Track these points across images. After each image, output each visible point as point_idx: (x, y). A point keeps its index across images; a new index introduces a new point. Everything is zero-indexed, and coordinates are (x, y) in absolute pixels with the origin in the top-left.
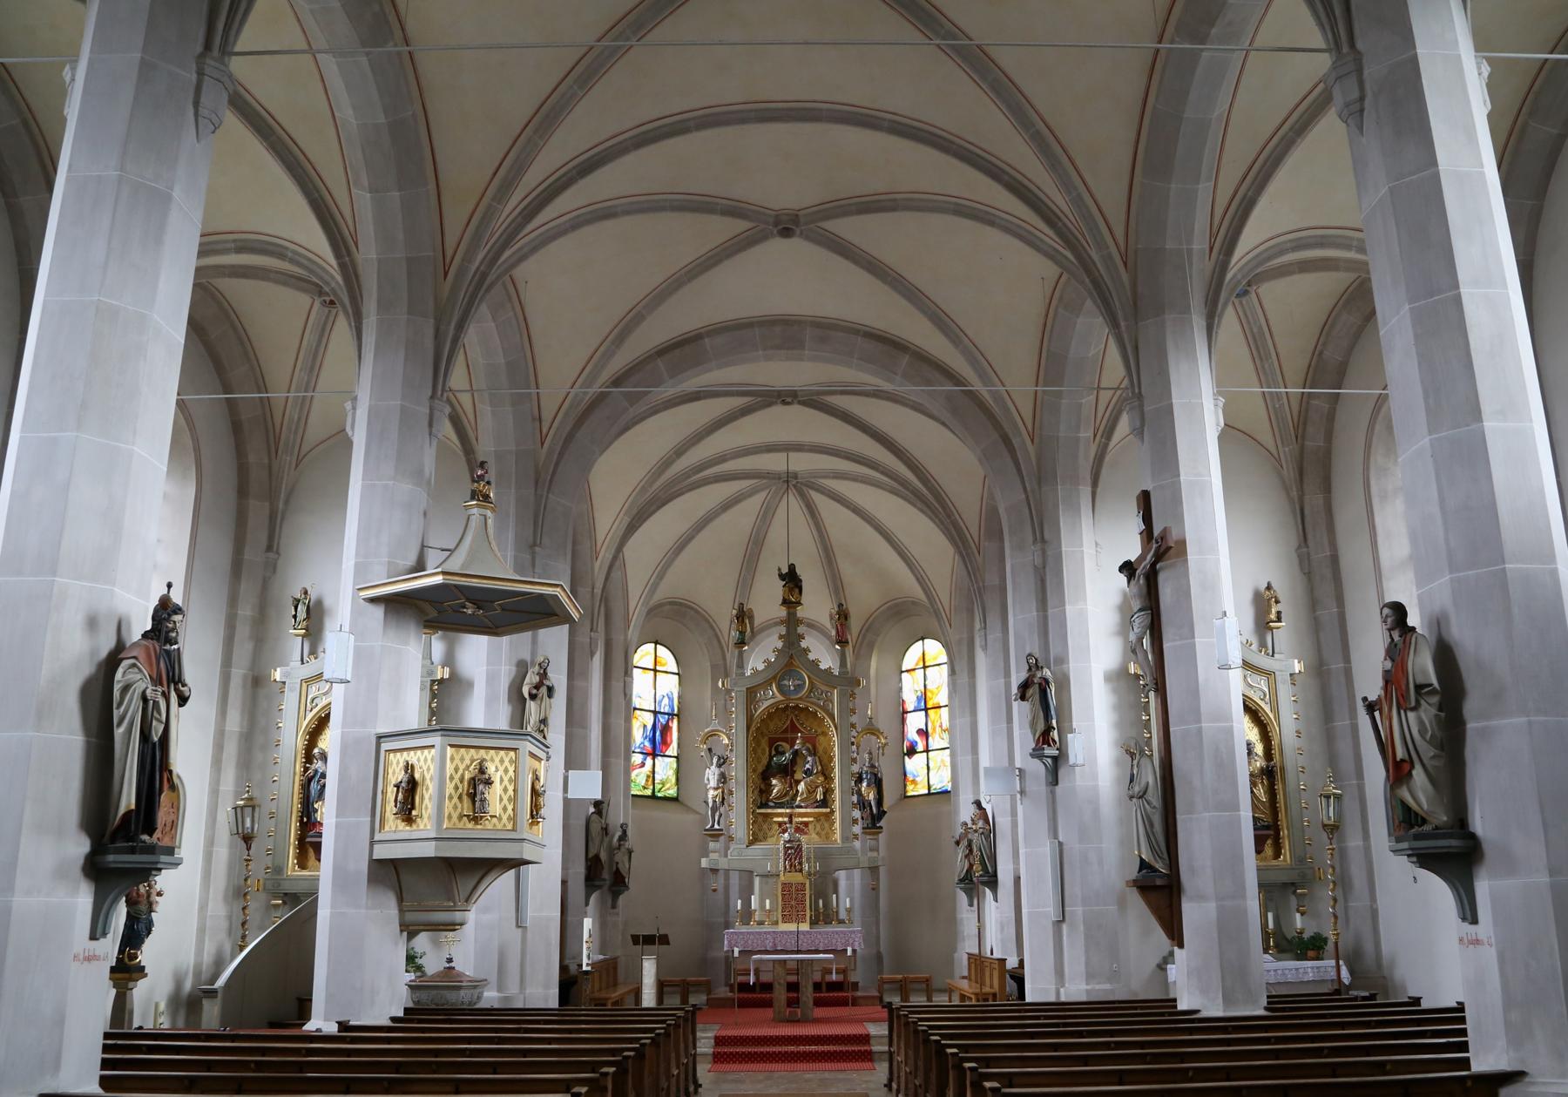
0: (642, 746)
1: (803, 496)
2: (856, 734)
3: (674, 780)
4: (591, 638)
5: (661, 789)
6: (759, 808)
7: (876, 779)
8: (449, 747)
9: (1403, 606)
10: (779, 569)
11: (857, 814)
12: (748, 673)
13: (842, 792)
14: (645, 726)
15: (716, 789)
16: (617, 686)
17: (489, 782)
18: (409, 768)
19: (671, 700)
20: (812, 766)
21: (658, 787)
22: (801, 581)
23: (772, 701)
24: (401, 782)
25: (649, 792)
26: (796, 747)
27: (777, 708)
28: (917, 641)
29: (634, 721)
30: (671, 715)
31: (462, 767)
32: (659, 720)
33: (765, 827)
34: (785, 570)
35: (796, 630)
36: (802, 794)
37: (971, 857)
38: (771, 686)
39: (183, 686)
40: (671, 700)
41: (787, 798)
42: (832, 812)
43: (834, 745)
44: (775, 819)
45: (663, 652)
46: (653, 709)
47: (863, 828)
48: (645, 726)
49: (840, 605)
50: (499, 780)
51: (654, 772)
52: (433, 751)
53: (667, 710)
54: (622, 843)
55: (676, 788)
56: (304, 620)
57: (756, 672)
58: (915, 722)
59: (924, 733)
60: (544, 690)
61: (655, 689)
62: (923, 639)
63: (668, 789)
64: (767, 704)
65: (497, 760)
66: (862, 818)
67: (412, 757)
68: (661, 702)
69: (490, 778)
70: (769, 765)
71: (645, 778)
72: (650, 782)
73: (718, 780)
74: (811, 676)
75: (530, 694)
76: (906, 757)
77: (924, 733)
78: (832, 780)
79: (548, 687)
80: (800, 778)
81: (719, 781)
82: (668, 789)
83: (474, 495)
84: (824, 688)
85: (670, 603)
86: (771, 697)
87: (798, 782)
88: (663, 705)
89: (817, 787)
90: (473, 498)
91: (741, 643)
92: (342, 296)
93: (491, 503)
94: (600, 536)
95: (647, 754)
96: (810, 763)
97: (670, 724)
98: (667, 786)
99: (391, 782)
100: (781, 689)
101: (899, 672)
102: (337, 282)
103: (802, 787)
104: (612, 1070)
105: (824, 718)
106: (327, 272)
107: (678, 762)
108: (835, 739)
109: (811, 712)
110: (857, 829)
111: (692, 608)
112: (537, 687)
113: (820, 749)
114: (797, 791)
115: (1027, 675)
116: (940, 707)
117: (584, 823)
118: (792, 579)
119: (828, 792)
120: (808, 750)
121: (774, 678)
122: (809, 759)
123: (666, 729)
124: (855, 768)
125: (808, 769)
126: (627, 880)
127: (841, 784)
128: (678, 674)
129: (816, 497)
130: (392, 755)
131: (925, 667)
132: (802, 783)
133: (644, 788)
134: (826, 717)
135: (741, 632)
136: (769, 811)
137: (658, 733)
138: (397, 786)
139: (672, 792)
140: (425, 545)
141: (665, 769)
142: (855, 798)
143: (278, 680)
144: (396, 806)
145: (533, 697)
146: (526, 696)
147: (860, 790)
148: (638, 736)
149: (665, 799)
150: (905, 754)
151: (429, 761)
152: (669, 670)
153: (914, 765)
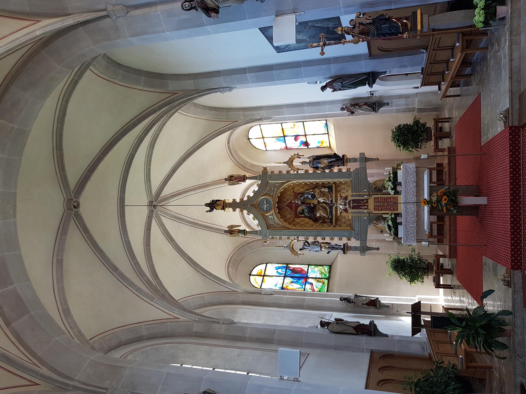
0: (301, 284)
1: (167, 199)
2: (293, 171)
3: (320, 267)
4: (223, 324)
5: (324, 274)
6: (332, 224)
7: (317, 159)
10: (207, 212)
11: (336, 170)
12: (260, 228)
13: (323, 178)
14: (292, 282)
15: (321, 248)
16: (266, 299)
20: (310, 194)
21: (323, 276)
23: (275, 217)
25: (326, 281)
26: (300, 203)
27: (278, 213)
28: (250, 142)
30: (287, 268)
32: (289, 275)
33: (343, 220)
34: (208, 209)
35: (238, 203)
36: (325, 200)
37: (361, 104)
38: (267, 216)
41: (327, 208)
42: (335, 183)
43: (298, 182)
44: (339, 214)
45: (254, 272)
46: (283, 278)
47: (344, 166)
48: (292, 282)
51: (315, 278)
54: (351, 301)
55: (324, 266)
57: (260, 224)
58: (291, 143)
59: (296, 137)
61: (273, 276)
62: (249, 139)
63: (325, 270)
64: (276, 219)
66: (338, 166)
68: (280, 273)
70: (309, 218)
72: (321, 280)
73: (316, 246)
77: (296, 137)
78: (317, 183)
80: (317, 200)
81: (317, 245)
82: (325, 270)
84: (268, 188)
85: (228, 268)
86: (272, 216)
88: (282, 272)
89: (321, 192)
94: (164, 316)
95: (306, 281)
96: (308, 195)
97: (292, 268)
98: (323, 270)
100: (268, 211)
101: (266, 152)
103: (321, 200)
105: (284, 188)
108: (295, 182)
109: (281, 194)
110: (344, 169)
111: (232, 257)
113: (302, 190)
114: (323, 202)
115: (199, 9)
116: (283, 129)
117: (334, 335)
118: (213, 205)
119: (324, 185)
120: (301, 197)
121: (262, 214)
122: (306, 196)
123: (294, 271)
124: (311, 171)
125: (311, 196)
126: (373, 299)
127: (319, 178)
128: (267, 264)
129: (167, 191)
131: (263, 138)
132: (319, 200)
133: (324, 283)
134: (283, 187)
135: (239, 232)
136: (334, 218)
137: (296, 275)
139: (327, 268)
141: (314, 272)
142: (327, 171)
147: (322, 168)
148: (296, 286)
149: (330, 272)
150: (308, 148)
152: (265, 269)
153: (313, 142)
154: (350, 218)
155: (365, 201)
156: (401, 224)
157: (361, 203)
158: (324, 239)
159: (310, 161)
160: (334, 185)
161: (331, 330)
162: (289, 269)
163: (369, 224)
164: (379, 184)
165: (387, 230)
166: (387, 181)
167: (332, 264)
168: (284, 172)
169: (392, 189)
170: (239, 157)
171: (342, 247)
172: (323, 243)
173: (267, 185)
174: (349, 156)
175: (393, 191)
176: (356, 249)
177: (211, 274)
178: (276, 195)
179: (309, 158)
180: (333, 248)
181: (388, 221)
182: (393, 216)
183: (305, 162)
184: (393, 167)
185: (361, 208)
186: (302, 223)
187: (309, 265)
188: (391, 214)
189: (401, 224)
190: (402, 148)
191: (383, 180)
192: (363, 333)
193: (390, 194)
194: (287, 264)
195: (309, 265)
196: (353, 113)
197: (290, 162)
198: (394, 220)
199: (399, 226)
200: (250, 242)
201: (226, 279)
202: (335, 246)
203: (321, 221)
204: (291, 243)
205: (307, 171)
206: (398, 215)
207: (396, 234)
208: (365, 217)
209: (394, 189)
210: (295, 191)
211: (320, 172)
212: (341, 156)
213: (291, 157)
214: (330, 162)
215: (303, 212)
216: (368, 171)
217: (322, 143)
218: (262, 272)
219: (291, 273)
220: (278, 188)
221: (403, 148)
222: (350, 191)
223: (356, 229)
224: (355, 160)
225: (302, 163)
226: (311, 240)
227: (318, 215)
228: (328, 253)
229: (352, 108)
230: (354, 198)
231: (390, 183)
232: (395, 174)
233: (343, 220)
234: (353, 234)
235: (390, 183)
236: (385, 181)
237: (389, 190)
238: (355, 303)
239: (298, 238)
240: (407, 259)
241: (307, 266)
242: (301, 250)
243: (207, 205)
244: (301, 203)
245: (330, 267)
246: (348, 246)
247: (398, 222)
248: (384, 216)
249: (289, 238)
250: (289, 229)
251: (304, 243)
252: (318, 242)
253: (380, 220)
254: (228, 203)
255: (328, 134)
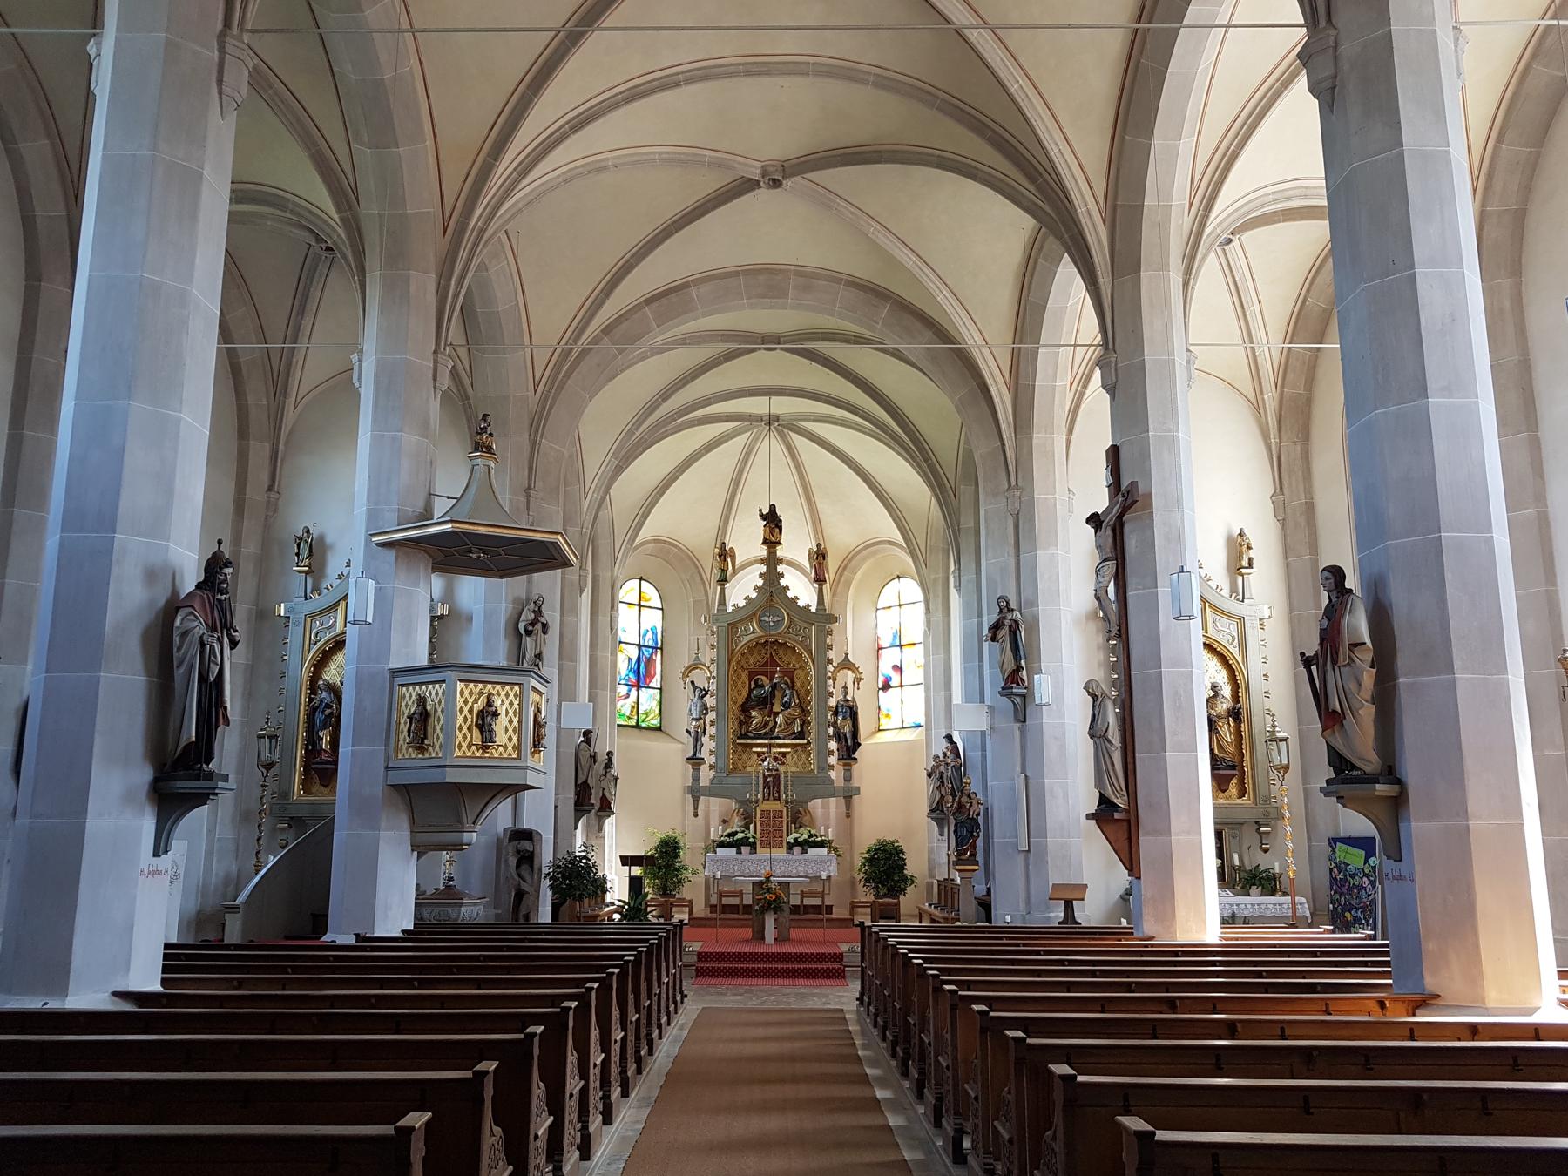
0: (627, 678)
1: (783, 437)
2: (832, 669)
3: (657, 711)
4: (580, 576)
6: (739, 738)
7: (851, 714)
8: (459, 683)
9: (1342, 569)
10: (760, 510)
11: (833, 745)
12: (730, 609)
13: (818, 724)
14: (630, 659)
15: (697, 720)
16: (603, 620)
17: (496, 714)
18: (421, 701)
19: (655, 634)
20: (790, 700)
21: (642, 717)
22: (781, 521)
24: (414, 714)
25: (633, 722)
26: (775, 681)
29: (620, 654)
30: (655, 648)
31: (471, 701)
33: (744, 757)
36: (780, 725)
37: (943, 789)
39: (234, 632)
40: (655, 634)
41: (767, 729)
42: (809, 743)
43: (811, 679)
44: (754, 749)
46: (637, 643)
47: (839, 760)
48: (630, 659)
49: (819, 545)
50: (504, 712)
51: (638, 703)
52: (444, 685)
53: (651, 643)
56: (307, 558)
57: (737, 609)
58: (889, 658)
59: (898, 669)
60: (539, 626)
63: (652, 719)
64: (747, 639)
65: (503, 694)
66: (838, 750)
67: (422, 690)
68: (645, 636)
69: (496, 710)
70: (749, 695)
71: (630, 709)
72: (635, 713)
74: (790, 613)
75: (526, 630)
76: (881, 691)
77: (898, 669)
79: (543, 623)
80: (779, 710)
81: (701, 712)
82: (652, 719)
83: (477, 447)
86: (752, 631)
87: (777, 714)
90: (476, 450)
91: (723, 580)
92: (344, 249)
93: (494, 454)
95: (633, 686)
97: (654, 657)
99: (403, 714)
101: (874, 609)
102: (339, 236)
103: (779, 719)
104: (617, 971)
105: (802, 653)
106: (329, 225)
107: (661, 693)
108: (812, 673)
110: (833, 760)
112: (533, 624)
113: (798, 684)
114: (776, 723)
118: (772, 520)
119: (805, 723)
120: (786, 683)
121: (754, 614)
122: (787, 692)
123: (650, 661)
124: (832, 702)
125: (786, 702)
128: (662, 609)
129: (797, 439)
130: (404, 689)
132: (781, 716)
133: (629, 718)
135: (723, 570)
136: (749, 741)
138: (410, 717)
139: (655, 722)
140: (432, 492)
141: (649, 699)
142: (831, 731)
143: (282, 614)
144: (409, 736)
145: (529, 633)
146: (523, 632)
147: (835, 722)
148: (623, 667)
151: (440, 694)
153: (888, 699)
154: (748, 769)
155: (776, 795)
156: (739, 852)
157: (774, 788)
158: (712, 724)
159: (848, 701)
160: (805, 741)
161: (581, 748)
162: (653, 652)
163: (738, 802)
164: (805, 818)
165: (729, 831)
166: (810, 831)
167: (665, 733)
168: (831, 654)
169: (796, 839)
170: (865, 559)
171: (698, 756)
172: (705, 723)
173: (808, 623)
174: (855, 768)
175: (792, 841)
176: (696, 778)
177: (645, 517)
178: (790, 639)
179: (853, 698)
180: (696, 740)
181: (743, 832)
182: (751, 840)
183: (846, 693)
184: (833, 841)
185: (764, 788)
186: (740, 684)
187: (660, 689)
188: (754, 838)
189: (739, 852)
190: (867, 856)
191: (812, 824)
192: (577, 794)
193: (788, 836)
194: (661, 649)
195: (660, 689)
196: (929, 775)
197: (847, 664)
198: (744, 842)
199: (735, 849)
200: (702, 579)
201: (639, 539)
202: (699, 743)
203: (742, 717)
204: (705, 665)
205: (831, 694)
206: (753, 847)
207: (722, 845)
208: (751, 795)
209: (797, 843)
210: (796, 672)
211: (829, 717)
212: (855, 756)
213: (857, 666)
214: (845, 736)
215: (759, 686)
216: (833, 800)
217: (887, 716)
218: (646, 601)
219: (646, 657)
220: (801, 643)
221: (865, 858)
222: (794, 769)
223: (730, 780)
224: (848, 779)
225: (845, 688)
226: (710, 701)
227: (754, 713)
228: (688, 731)
229: (937, 774)
230: (782, 776)
231: (805, 836)
232: (821, 845)
233: (744, 757)
234: (720, 775)
235: (805, 836)
236: (809, 829)
237: (794, 835)
238: (605, 776)
239: (714, 678)
240: (680, 862)
241: (659, 686)
242: (692, 682)
243: (773, 508)
244: (776, 683)
245: (659, 729)
246: (700, 765)
247: (742, 848)
248: (752, 826)
249: (712, 662)
250: (729, 662)
251: (704, 690)
252: (706, 714)
253: (745, 819)
254: (776, 551)
255: (903, 728)
